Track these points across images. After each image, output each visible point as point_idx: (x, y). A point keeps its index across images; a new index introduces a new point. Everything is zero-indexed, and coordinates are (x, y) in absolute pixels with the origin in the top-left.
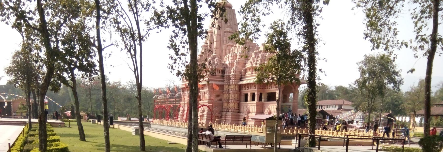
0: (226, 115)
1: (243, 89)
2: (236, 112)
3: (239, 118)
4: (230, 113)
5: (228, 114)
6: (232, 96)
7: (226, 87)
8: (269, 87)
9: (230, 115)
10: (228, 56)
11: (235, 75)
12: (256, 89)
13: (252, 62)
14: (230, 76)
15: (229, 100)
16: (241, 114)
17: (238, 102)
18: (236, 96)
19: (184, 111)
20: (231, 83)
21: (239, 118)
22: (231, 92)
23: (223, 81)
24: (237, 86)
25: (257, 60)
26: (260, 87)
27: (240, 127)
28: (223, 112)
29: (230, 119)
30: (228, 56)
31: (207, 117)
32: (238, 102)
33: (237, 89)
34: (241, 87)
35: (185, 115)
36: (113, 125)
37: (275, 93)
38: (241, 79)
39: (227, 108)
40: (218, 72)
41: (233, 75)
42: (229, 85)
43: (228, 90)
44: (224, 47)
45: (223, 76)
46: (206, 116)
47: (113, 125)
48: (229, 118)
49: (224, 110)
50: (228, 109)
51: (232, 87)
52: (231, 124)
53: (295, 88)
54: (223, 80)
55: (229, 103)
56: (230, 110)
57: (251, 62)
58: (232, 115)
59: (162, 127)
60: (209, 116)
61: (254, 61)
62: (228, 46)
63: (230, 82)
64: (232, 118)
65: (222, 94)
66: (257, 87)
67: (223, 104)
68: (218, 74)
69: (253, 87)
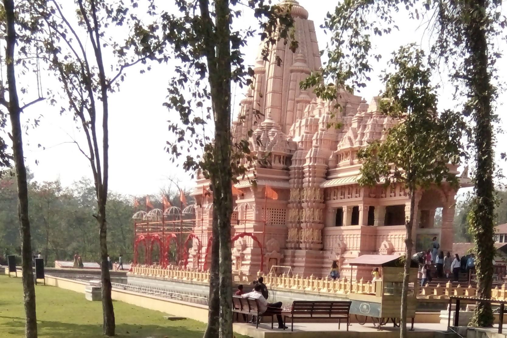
0: (294, 256)
1: (332, 197)
2: (315, 249)
3: (323, 263)
4: (303, 252)
5: (299, 252)
6: (306, 213)
7: (294, 194)
8: (388, 193)
9: (302, 257)
10: (297, 124)
11: (314, 167)
12: (361, 199)
14: (303, 168)
15: (300, 222)
16: (328, 254)
17: (321, 226)
18: (317, 213)
19: (200, 247)
20: (305, 185)
21: (323, 263)
22: (304, 205)
23: (288, 180)
24: (318, 192)
25: (363, 134)
26: (370, 193)
27: (326, 282)
28: (287, 248)
30: (297, 124)
32: (321, 226)
33: (318, 199)
34: (326, 193)
35: (204, 256)
36: (42, 277)
37: (404, 206)
38: (327, 176)
39: (296, 240)
40: (277, 161)
41: (309, 167)
42: (301, 189)
43: (298, 200)
44: (290, 104)
45: (288, 169)
47: (42, 277)
49: (289, 245)
50: (299, 242)
51: (307, 194)
52: (306, 276)
53: (447, 197)
54: (287, 177)
55: (300, 229)
56: (302, 245)
57: (350, 139)
59: (153, 283)
60: (255, 257)
61: (356, 137)
62: (298, 102)
63: (302, 183)
64: (306, 262)
65: (286, 208)
66: (362, 194)
67: (287, 231)
68: (277, 164)
69: (354, 194)
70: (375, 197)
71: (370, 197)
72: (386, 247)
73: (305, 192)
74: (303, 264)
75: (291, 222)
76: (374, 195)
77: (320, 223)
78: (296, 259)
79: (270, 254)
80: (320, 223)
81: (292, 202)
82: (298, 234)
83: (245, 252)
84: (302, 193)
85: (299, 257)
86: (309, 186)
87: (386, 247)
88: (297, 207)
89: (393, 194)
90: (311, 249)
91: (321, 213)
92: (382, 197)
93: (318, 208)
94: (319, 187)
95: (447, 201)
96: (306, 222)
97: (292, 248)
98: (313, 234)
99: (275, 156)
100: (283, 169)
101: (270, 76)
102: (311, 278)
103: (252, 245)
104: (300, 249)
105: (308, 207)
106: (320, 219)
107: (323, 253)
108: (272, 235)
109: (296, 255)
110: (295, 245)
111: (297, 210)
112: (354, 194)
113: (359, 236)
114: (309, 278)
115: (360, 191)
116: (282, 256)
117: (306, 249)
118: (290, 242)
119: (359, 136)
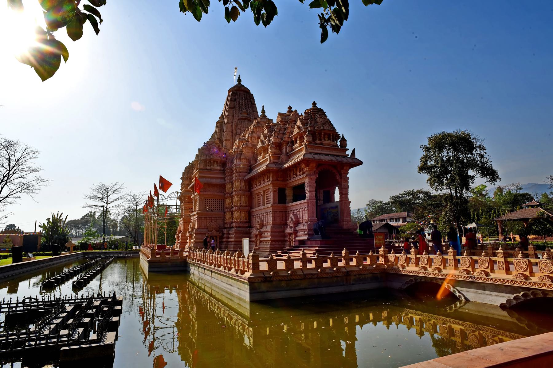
0: (229, 234)
2: (244, 227)
7: (228, 187)
13: (263, 139)
17: (247, 209)
18: (243, 199)
24: (243, 183)
28: (225, 228)
29: (269, 239)
32: (247, 209)
33: (243, 188)
37: (303, 184)
40: (215, 165)
45: (224, 171)
49: (226, 226)
53: (341, 175)
66: (271, 179)
70: (282, 181)
71: (277, 180)
76: (281, 179)
77: (246, 206)
80: (246, 206)
86: (236, 180)
90: (240, 227)
91: (247, 199)
94: (243, 180)
95: (341, 178)
98: (240, 215)
99: (214, 162)
100: (220, 170)
105: (236, 195)
106: (246, 203)
107: (250, 230)
109: (230, 232)
116: (221, 234)
117: (236, 227)
118: (227, 223)
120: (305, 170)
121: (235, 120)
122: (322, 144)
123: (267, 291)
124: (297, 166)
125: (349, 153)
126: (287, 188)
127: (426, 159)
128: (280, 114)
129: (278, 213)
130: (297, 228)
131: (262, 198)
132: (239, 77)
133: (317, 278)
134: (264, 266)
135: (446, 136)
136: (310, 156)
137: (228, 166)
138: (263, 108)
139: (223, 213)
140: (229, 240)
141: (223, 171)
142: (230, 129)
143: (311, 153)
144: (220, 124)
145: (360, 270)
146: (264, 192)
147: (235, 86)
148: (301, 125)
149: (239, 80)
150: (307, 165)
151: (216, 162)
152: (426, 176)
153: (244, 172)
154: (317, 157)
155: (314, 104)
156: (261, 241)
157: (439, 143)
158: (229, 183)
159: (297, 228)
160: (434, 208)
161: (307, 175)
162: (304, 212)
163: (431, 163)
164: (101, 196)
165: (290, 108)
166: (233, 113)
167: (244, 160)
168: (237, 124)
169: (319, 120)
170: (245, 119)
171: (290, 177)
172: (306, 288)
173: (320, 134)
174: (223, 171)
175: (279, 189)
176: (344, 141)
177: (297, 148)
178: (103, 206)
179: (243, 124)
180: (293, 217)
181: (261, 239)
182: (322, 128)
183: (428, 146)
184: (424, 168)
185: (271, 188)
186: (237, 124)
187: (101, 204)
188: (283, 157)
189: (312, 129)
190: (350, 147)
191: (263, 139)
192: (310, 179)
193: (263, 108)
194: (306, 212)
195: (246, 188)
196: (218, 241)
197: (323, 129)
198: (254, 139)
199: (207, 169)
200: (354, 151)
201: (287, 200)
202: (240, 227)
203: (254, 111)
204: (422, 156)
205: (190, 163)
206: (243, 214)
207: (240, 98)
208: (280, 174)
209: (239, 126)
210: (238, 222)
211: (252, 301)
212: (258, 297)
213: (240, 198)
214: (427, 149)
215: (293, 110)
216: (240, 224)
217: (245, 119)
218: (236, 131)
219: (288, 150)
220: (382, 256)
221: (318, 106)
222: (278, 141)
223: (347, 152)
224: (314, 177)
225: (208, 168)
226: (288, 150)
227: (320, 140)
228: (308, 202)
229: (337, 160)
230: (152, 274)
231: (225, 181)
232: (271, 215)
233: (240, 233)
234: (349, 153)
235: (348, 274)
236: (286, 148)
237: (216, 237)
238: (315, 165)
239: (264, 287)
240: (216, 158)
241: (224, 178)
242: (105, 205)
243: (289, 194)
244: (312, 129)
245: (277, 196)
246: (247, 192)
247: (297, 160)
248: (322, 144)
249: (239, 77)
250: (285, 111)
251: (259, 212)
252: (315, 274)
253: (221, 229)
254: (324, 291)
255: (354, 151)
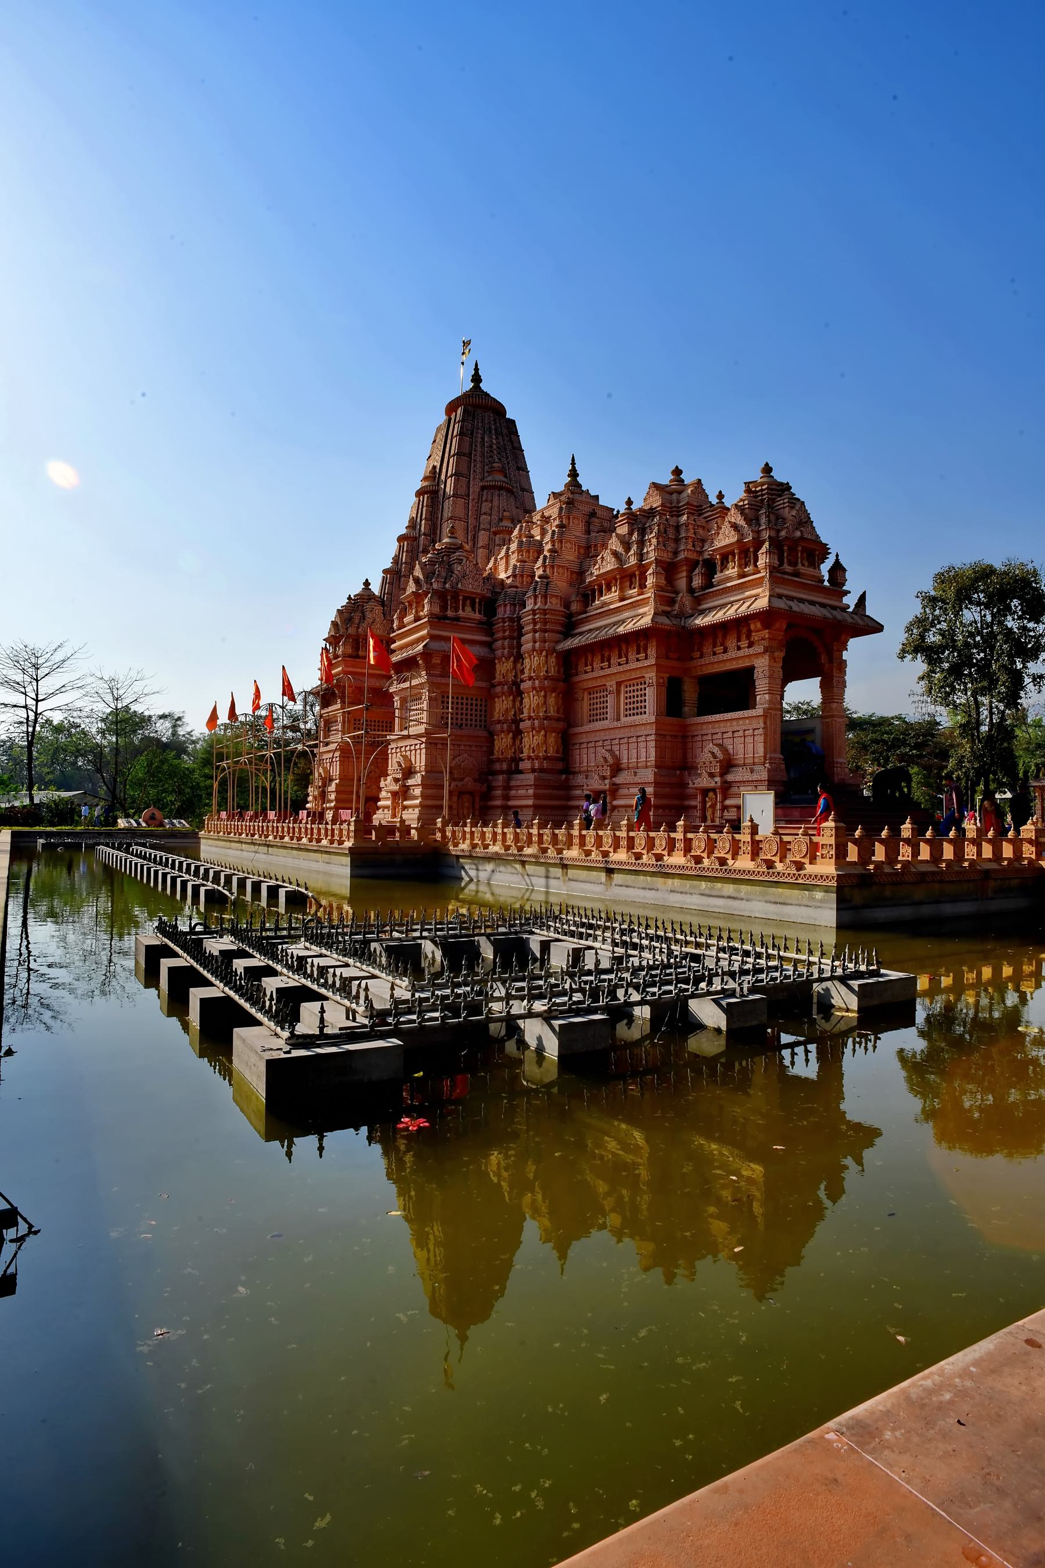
0: (507, 787)
1: (581, 668)
4: (530, 778)
5: (518, 779)
6: (531, 701)
7: (503, 668)
8: (707, 649)
9: (526, 787)
10: (503, 553)
11: (544, 612)
12: (652, 661)
13: (620, 549)
14: (519, 618)
15: (517, 721)
16: (580, 779)
17: (561, 725)
18: (552, 700)
20: (527, 647)
24: (552, 660)
25: (641, 543)
30: (503, 553)
31: (423, 795)
32: (561, 725)
33: (552, 673)
37: (751, 669)
38: (569, 626)
39: (510, 754)
40: (468, 609)
42: (519, 657)
43: (510, 678)
44: (483, 537)
46: (417, 791)
48: (525, 796)
49: (497, 766)
50: (516, 760)
51: (532, 663)
55: (518, 733)
57: (615, 554)
58: (536, 786)
61: (627, 547)
62: (495, 533)
63: (519, 645)
64: (536, 796)
65: (489, 697)
66: (652, 652)
67: (491, 735)
71: (668, 658)
72: (715, 757)
73: (527, 661)
74: (530, 802)
75: (499, 722)
77: (558, 720)
78: (513, 792)
79: (460, 784)
80: (558, 720)
81: (500, 683)
82: (514, 744)
83: (410, 782)
84: (519, 666)
85: (518, 787)
86: (534, 649)
87: (715, 757)
88: (511, 693)
89: (719, 649)
91: (560, 701)
92: (692, 659)
93: (553, 690)
94: (554, 650)
95: (831, 660)
96: (530, 718)
97: (502, 772)
98: (545, 742)
100: (480, 622)
101: (452, 452)
102: (680, 829)
103: (423, 768)
104: (521, 772)
105: (534, 688)
107: (567, 779)
108: (462, 747)
110: (510, 766)
111: (511, 698)
112: (632, 656)
113: (653, 737)
114: (570, 826)
115: (645, 651)
117: (533, 770)
118: (498, 760)
119: (635, 547)
120: (755, 637)
121: (475, 489)
122: (797, 574)
123: (866, 906)
124: (739, 626)
125: (850, 601)
126: (686, 679)
127: (922, 624)
128: (655, 486)
129: (668, 738)
130: (730, 778)
131: (610, 699)
132: (476, 369)
133: (941, 882)
134: (853, 853)
135: (985, 573)
136: (781, 604)
137: (503, 612)
138: (573, 463)
139: (485, 734)
140: (511, 803)
141: (487, 627)
142: (460, 512)
143: (780, 596)
144: (431, 493)
145: (1004, 870)
146: (619, 684)
147: (466, 396)
148: (740, 521)
149: (477, 379)
150: (766, 626)
151: (470, 599)
152: (920, 666)
153: (552, 631)
154: (796, 607)
155: (767, 470)
156: (614, 808)
157: (962, 587)
158: (508, 659)
159: (730, 778)
160: (889, 750)
161: (766, 650)
162: (749, 740)
163: (933, 638)
164: (19, 677)
165: (677, 472)
166: (469, 468)
167: (554, 600)
168: (480, 501)
169: (788, 514)
170: (501, 488)
171: (700, 650)
172: (921, 903)
173: (793, 550)
174: (487, 627)
175: (669, 679)
176: (838, 569)
177: (729, 579)
178: (26, 707)
179: (496, 503)
180: (716, 750)
181: (615, 803)
182: (798, 534)
183: (933, 593)
184: (917, 647)
185: (651, 676)
186: (480, 501)
187: (20, 700)
188: (684, 600)
189: (773, 534)
190: (853, 587)
191: (620, 549)
192: (773, 659)
193: (573, 463)
194: (761, 739)
195: (558, 672)
196: (477, 806)
197: (802, 538)
198: (568, 545)
199: (446, 618)
200: (862, 598)
201: (686, 709)
202: (542, 770)
203: (519, 469)
204: (911, 618)
205: (349, 598)
206: (552, 739)
207: (481, 429)
208: (675, 640)
209: (485, 507)
210: (537, 758)
211: (840, 927)
212: (848, 916)
213: (545, 697)
214: (932, 601)
215: (688, 478)
216: (545, 765)
217: (501, 488)
218: (477, 518)
219: (697, 582)
220: (1030, 841)
221: (779, 476)
222: (666, 557)
223: (846, 600)
224: (780, 655)
225: (450, 613)
226: (697, 582)
227: (793, 563)
228: (765, 716)
229: (835, 618)
230: (359, 881)
231: (493, 651)
232: (653, 744)
233: (546, 787)
234: (850, 601)
235: (936, 877)
236: (690, 580)
237: (472, 794)
238: (784, 627)
239: (858, 897)
240: (470, 588)
241: (489, 645)
242: (31, 703)
243: (690, 693)
244: (773, 534)
245: (664, 696)
246: (561, 684)
247: (743, 609)
248: (797, 574)
249: (476, 369)
250: (665, 479)
251: (593, 738)
252: (933, 873)
253: (486, 773)
254: (948, 909)
255: (862, 598)
